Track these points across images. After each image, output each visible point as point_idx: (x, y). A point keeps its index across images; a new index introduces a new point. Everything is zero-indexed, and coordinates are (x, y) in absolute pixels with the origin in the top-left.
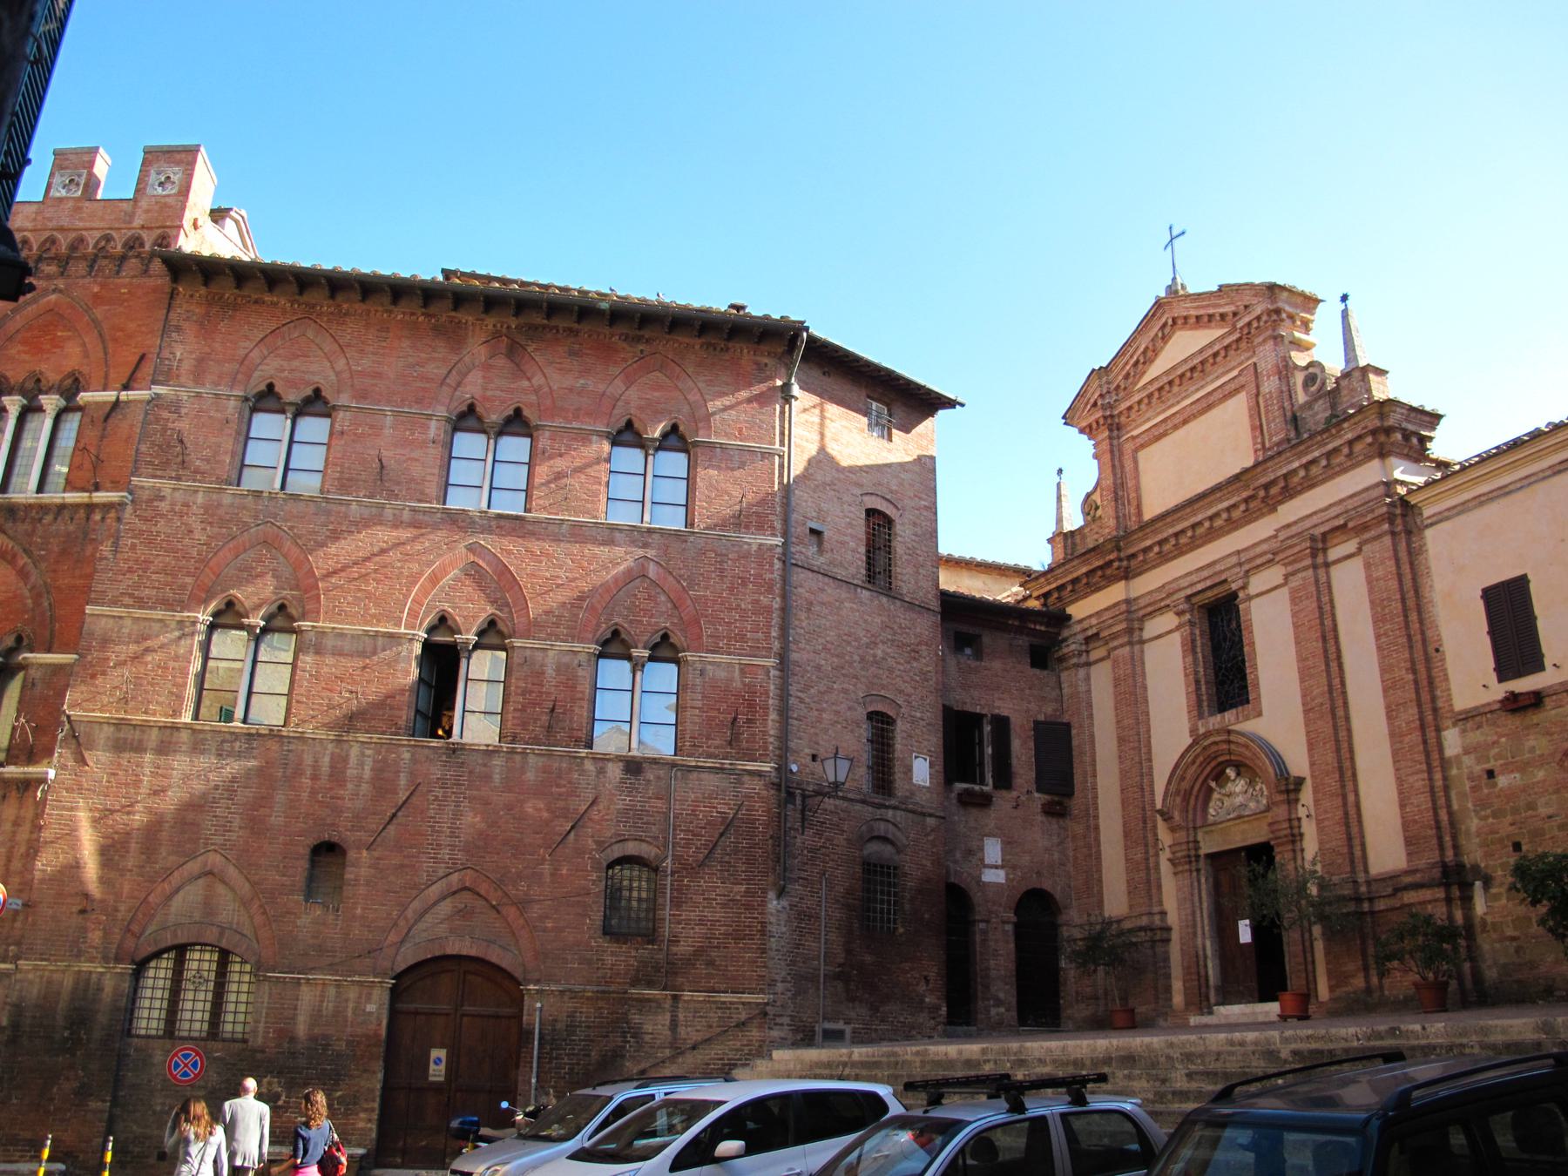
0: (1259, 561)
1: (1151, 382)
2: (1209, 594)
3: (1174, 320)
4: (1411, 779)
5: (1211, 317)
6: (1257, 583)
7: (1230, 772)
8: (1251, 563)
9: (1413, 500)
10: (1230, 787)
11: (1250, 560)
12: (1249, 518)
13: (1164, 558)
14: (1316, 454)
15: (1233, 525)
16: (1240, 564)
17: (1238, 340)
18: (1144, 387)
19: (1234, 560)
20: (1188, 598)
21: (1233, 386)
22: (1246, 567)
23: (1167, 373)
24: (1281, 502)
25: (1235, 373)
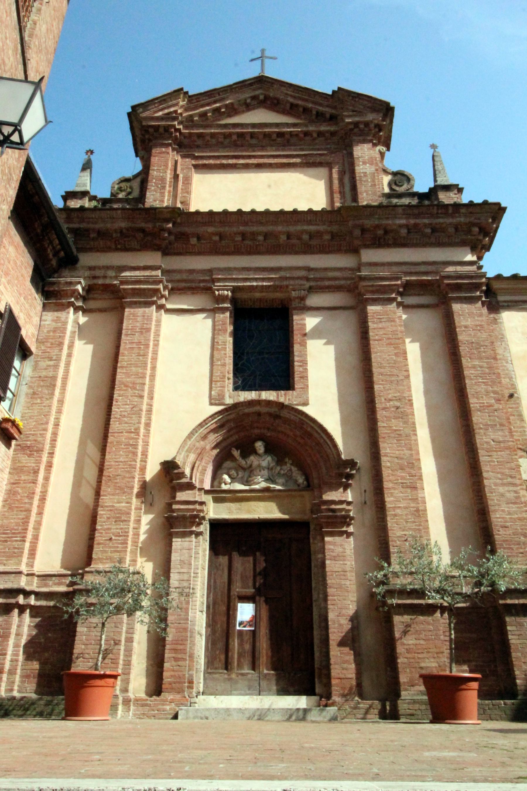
0: (327, 283)
1: (235, 125)
2: (258, 295)
3: (266, 98)
4: (501, 489)
5: (306, 110)
6: (314, 300)
7: (260, 446)
8: (319, 283)
9: (496, 285)
10: (253, 460)
11: (315, 279)
12: (324, 250)
13: (216, 251)
14: (426, 221)
15: (307, 249)
16: (308, 279)
17: (333, 134)
18: (226, 126)
19: (303, 273)
20: (235, 290)
21: (318, 160)
22: (312, 284)
23: (254, 126)
24: (367, 246)
25: (325, 152)
